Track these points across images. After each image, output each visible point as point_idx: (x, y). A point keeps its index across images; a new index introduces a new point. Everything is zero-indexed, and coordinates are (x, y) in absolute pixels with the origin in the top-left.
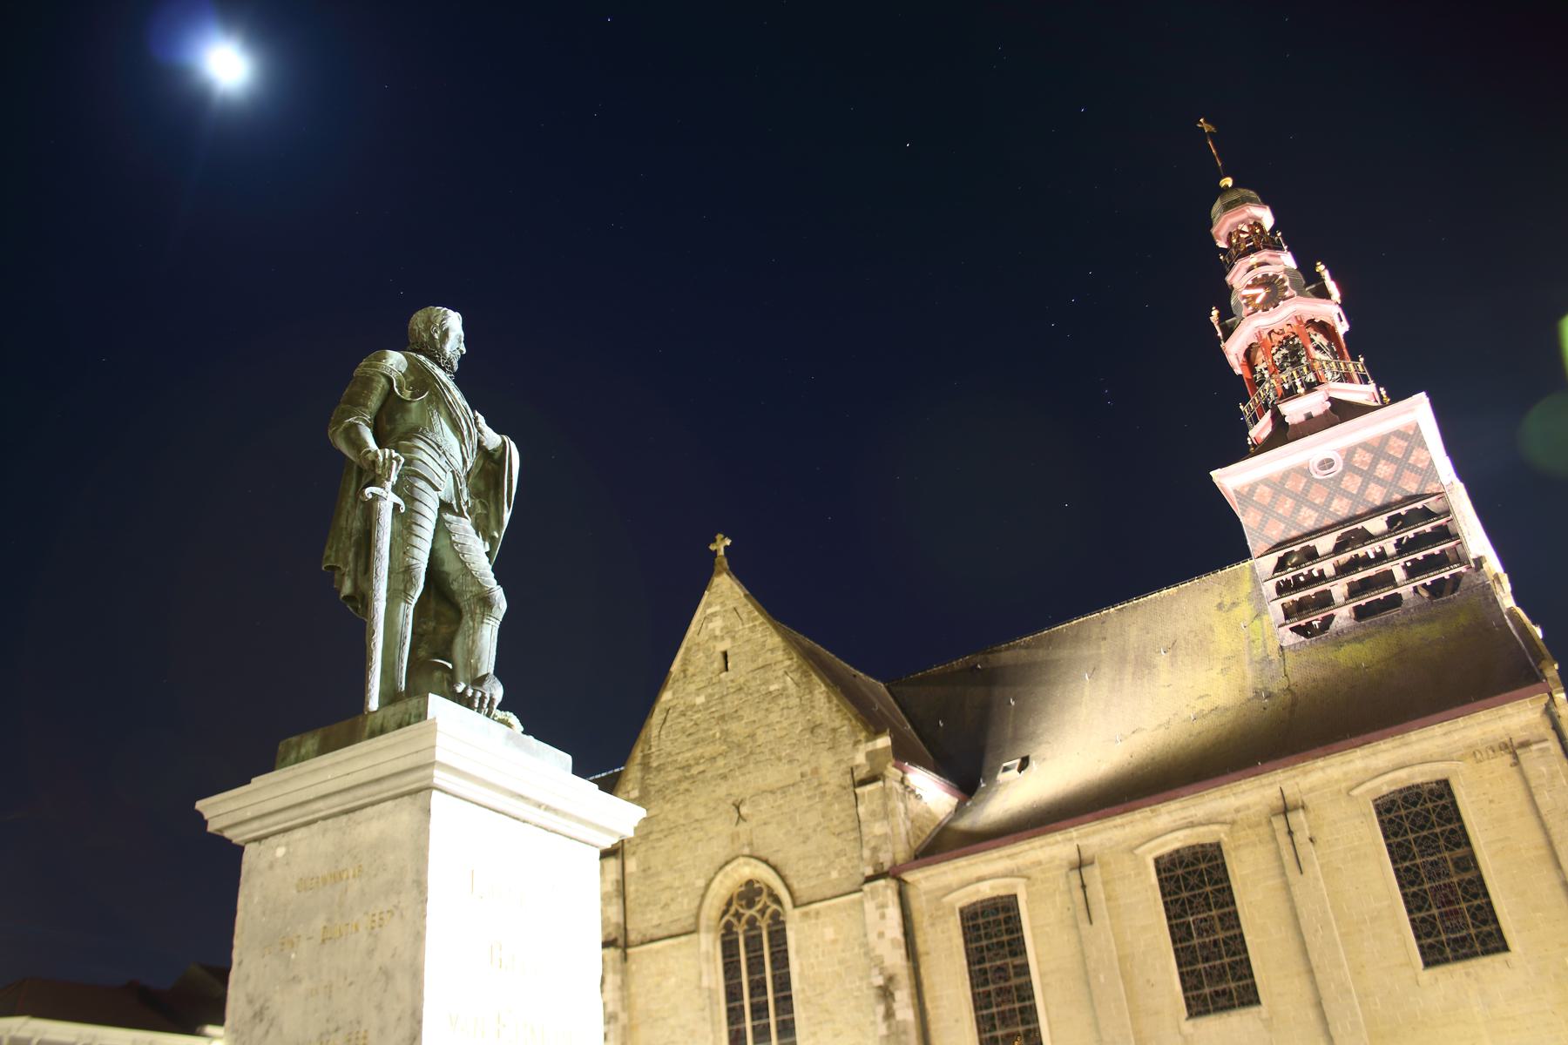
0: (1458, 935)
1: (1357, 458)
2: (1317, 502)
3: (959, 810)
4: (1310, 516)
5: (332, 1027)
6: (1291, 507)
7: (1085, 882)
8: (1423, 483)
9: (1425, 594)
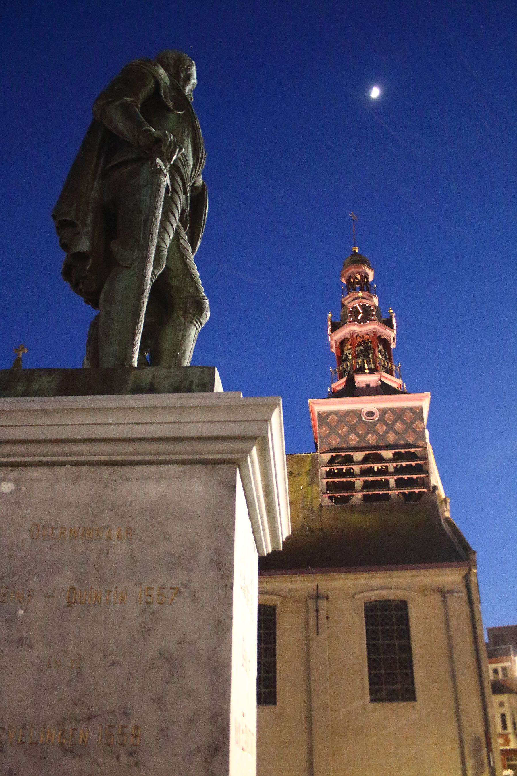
1: (387, 415)
2: (360, 432)
4: (355, 439)
5: (81, 712)
6: (346, 431)
8: (416, 439)
9: (402, 498)
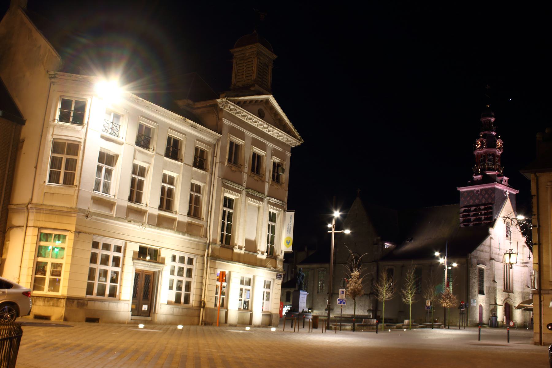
1: (483, 192)
3: (397, 248)
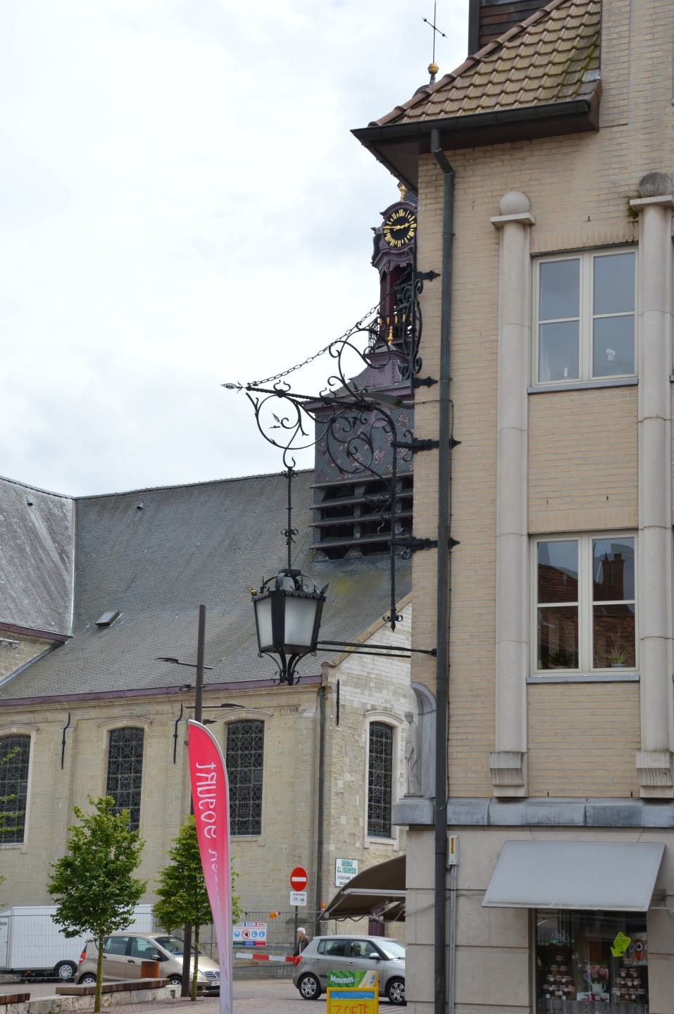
0: (244, 819)
7: (66, 740)
